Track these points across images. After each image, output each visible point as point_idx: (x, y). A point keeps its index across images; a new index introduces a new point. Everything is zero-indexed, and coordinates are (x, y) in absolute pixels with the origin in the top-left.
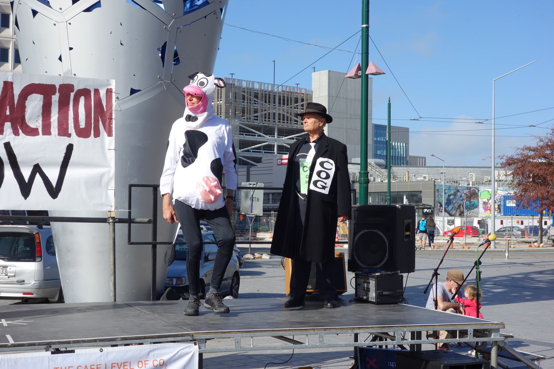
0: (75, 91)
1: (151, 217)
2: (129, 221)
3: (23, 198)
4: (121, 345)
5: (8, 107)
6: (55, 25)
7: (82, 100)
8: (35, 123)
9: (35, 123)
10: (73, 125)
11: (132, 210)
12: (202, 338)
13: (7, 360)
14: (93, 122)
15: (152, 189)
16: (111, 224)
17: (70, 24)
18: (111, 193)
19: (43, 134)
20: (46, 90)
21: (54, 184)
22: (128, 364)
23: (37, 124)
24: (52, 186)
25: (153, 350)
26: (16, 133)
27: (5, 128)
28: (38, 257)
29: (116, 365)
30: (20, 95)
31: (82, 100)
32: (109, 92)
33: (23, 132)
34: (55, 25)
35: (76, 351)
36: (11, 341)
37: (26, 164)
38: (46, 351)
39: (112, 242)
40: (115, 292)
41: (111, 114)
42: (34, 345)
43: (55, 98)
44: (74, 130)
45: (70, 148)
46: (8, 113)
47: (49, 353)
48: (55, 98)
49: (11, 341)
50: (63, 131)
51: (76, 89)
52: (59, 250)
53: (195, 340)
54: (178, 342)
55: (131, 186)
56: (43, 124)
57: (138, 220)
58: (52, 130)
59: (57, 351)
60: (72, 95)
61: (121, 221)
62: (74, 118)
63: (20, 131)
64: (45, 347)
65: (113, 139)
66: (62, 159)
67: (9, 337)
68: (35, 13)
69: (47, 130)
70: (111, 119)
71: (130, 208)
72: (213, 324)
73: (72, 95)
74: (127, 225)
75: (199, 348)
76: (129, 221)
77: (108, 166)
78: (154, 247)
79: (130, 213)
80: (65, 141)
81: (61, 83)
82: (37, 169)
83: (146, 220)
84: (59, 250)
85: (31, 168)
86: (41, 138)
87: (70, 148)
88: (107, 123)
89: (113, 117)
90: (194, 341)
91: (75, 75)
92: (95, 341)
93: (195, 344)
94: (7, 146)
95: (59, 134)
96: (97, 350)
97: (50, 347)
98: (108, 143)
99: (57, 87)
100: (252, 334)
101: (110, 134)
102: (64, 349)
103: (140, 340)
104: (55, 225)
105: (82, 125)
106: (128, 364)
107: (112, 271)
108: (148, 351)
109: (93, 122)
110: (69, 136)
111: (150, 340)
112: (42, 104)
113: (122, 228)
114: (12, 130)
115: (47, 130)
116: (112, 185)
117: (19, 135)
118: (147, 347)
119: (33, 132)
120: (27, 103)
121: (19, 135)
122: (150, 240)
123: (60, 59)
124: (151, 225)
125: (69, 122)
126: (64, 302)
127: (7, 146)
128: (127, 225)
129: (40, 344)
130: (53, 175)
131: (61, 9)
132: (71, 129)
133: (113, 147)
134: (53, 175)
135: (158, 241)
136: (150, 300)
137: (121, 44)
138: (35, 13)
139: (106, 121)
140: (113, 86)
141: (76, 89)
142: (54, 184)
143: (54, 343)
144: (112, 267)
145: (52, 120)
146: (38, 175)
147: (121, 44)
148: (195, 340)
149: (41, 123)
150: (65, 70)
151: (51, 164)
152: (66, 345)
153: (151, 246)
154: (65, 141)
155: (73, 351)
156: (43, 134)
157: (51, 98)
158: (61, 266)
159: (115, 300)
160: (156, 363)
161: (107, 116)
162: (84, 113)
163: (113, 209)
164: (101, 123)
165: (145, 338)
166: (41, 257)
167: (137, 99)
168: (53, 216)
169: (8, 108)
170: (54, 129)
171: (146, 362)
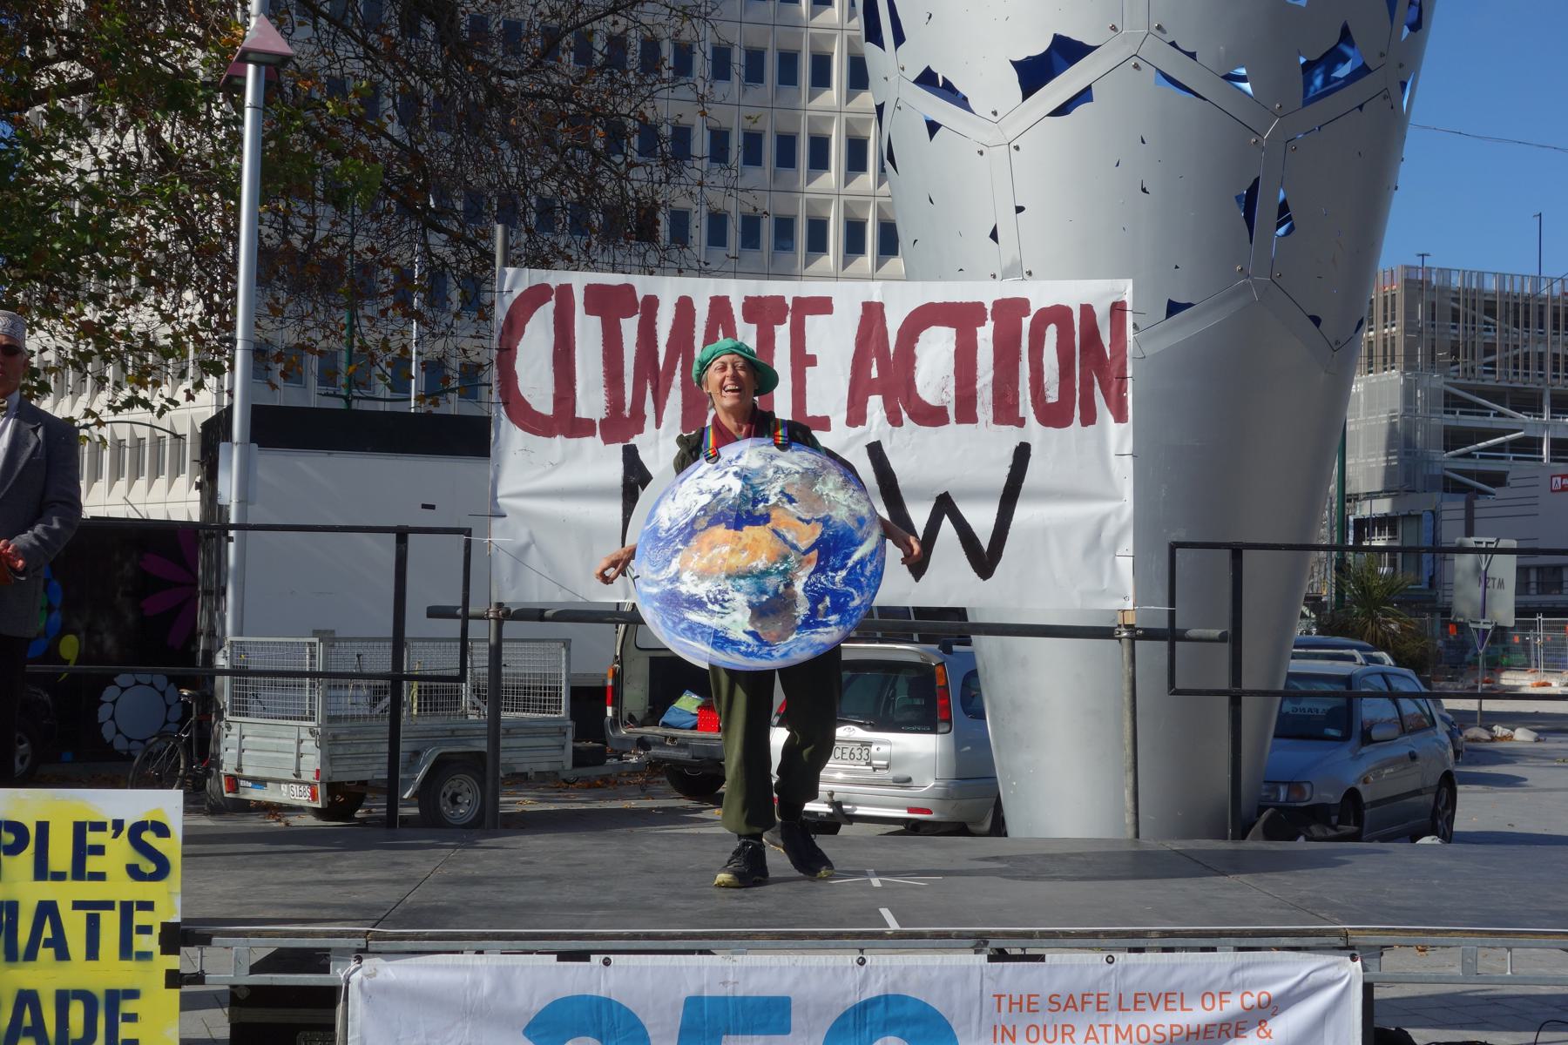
0: (1033, 313)
1: (1227, 628)
2: (1171, 635)
3: (910, 577)
4: (1152, 949)
5: (875, 360)
6: (981, 153)
7: (1051, 332)
10: (1029, 398)
11: (1177, 609)
12: (1372, 943)
13: (885, 968)
14: (1077, 386)
15: (1227, 553)
16: (1125, 641)
17: (1017, 148)
18: (1126, 564)
19: (958, 422)
20: (962, 317)
21: (985, 542)
22: (1177, 998)
24: (980, 547)
25: (1243, 967)
26: (895, 421)
28: (943, 721)
29: (1146, 998)
30: (900, 332)
31: (1051, 332)
32: (1118, 309)
33: (911, 416)
34: (981, 153)
35: (1048, 957)
36: (894, 926)
37: (919, 496)
38: (976, 952)
39: (1126, 687)
40: (1137, 814)
41: (1123, 366)
42: (947, 935)
43: (985, 334)
44: (1031, 410)
45: (1022, 454)
46: (874, 373)
47: (983, 958)
48: (985, 334)
49: (894, 926)
50: (1006, 413)
51: (1034, 309)
52: (994, 707)
53: (1352, 948)
54: (1306, 949)
55: (1174, 547)
56: (957, 397)
57: (1193, 633)
58: (979, 411)
59: (1000, 956)
60: (1026, 322)
61: (1150, 635)
62: (1031, 380)
63: (905, 415)
64: (972, 942)
65: (1128, 427)
66: (1002, 480)
67: (886, 913)
68: (933, 127)
69: (967, 413)
70: (1123, 378)
71: (1172, 603)
72: (1398, 908)
73: (1026, 322)
74: (1165, 644)
75: (1365, 969)
76: (1171, 635)
77: (1118, 497)
78: (1236, 702)
79: (1172, 615)
80: (1010, 437)
81: (999, 297)
82: (945, 505)
83: (1216, 633)
84: (994, 707)
85: (932, 503)
86: (952, 429)
87: (1022, 454)
88: (1113, 389)
89: (1129, 373)
90: (1349, 949)
91: (1030, 273)
92: (1095, 935)
93: (1353, 958)
94: (875, 451)
95: (997, 420)
96: (1099, 958)
97: (986, 943)
98: (1116, 438)
99: (989, 307)
100: (1510, 941)
101: (1120, 417)
102: (1018, 952)
103: (1206, 941)
104: (985, 646)
105: (1052, 395)
106: (1177, 998)
107: (1128, 762)
108: (1228, 968)
109: (1077, 386)
110: (1021, 423)
111: (1234, 941)
112: (953, 347)
113: (1153, 654)
115: (967, 413)
116: (1128, 545)
118: (1224, 960)
119: (931, 416)
120: (919, 349)
121: (901, 424)
122: (1225, 684)
123: (994, 235)
124: (1225, 649)
125: (1020, 389)
126: (1006, 835)
127: (875, 451)
128: (1165, 644)
129: (960, 936)
130: (982, 519)
131: (995, 113)
132: (1026, 408)
133: (1128, 447)
134: (982, 519)
135: (1247, 684)
136: (1225, 838)
137: (1144, 190)
138: (933, 127)
139: (1110, 384)
140: (1128, 298)
141: (1034, 309)
142: (985, 542)
143: (995, 935)
144: (1128, 750)
145: (979, 386)
146: (946, 523)
147: (1144, 190)
148: (1352, 948)
149: (953, 394)
150: (1007, 262)
151: (977, 495)
152: (1023, 942)
153: (1226, 699)
154: (1010, 437)
155: (1041, 958)
156: (958, 422)
157: (975, 334)
158: (998, 747)
159: (1137, 835)
160: (1250, 1001)
161: (1114, 370)
162: (1056, 365)
163: (1129, 605)
164: (1097, 389)
165: (1221, 934)
166: (949, 721)
167: (1185, 329)
168: (980, 620)
170: (984, 408)
171: (1225, 997)
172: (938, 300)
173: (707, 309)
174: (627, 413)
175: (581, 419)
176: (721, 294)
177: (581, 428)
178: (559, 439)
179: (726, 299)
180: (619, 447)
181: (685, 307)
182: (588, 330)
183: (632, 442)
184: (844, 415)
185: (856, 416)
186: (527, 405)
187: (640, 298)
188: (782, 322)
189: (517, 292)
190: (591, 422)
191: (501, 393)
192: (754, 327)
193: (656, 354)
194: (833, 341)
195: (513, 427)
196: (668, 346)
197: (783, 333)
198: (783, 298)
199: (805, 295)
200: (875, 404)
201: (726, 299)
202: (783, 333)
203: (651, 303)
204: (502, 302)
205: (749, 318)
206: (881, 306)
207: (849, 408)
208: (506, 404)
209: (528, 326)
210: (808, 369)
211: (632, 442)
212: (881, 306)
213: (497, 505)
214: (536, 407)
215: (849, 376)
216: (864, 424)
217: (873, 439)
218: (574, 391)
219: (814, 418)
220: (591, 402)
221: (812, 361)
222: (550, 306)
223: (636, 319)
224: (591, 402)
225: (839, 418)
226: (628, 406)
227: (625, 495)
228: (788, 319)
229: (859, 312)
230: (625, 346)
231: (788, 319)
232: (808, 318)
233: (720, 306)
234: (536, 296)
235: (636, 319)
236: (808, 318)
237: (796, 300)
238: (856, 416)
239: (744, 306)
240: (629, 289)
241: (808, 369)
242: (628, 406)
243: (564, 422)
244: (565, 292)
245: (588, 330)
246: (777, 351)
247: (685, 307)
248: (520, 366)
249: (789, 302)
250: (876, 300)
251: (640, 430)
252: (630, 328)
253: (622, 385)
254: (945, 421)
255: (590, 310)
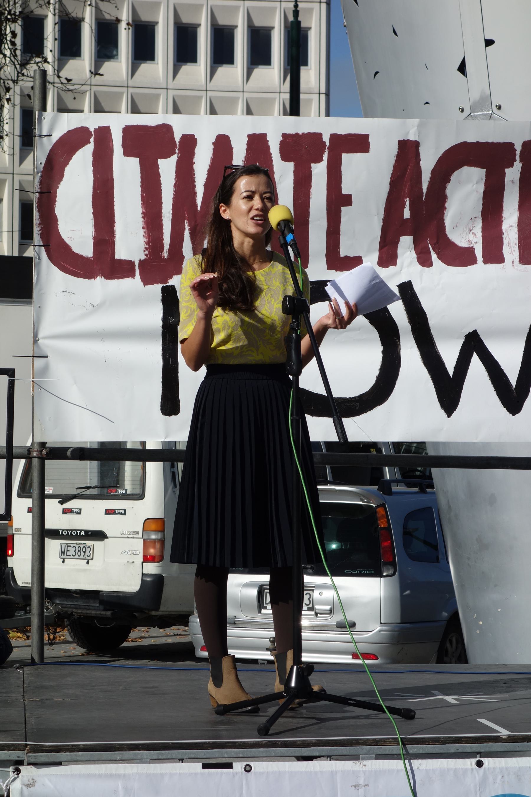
5: (407, 200)
8: (465, 233)
9: (465, 233)
23: (471, 237)
26: (424, 261)
27: (400, 251)
46: (407, 214)
63: (434, 256)
69: (494, 254)
114: (415, 255)
115: (494, 254)
117: (430, 265)
121: (430, 265)
169: (407, 204)
172: (471, 139)
173: (245, 146)
174: (165, 254)
175: (120, 261)
176: (258, 132)
177: (120, 270)
178: (100, 280)
179: (264, 136)
180: (157, 289)
181: (222, 144)
182: (126, 171)
183: (171, 282)
184: (375, 256)
185: (388, 257)
186: (67, 247)
187: (177, 138)
188: (319, 160)
189: (56, 136)
190: (131, 264)
191: (42, 236)
192: (291, 166)
193: (194, 194)
194: (367, 177)
195: (56, 271)
196: (206, 186)
197: (319, 171)
198: (320, 135)
199: (341, 131)
200: (406, 242)
201: (264, 136)
202: (319, 171)
203: (189, 142)
204: (42, 144)
205: (285, 157)
206: (416, 144)
207: (381, 249)
208: (46, 246)
209: (68, 170)
210: (343, 209)
211: (171, 282)
212: (416, 144)
213: (38, 347)
214: (76, 249)
215: (382, 216)
216: (395, 264)
217: (404, 279)
218: (113, 232)
219: (347, 258)
220: (130, 243)
221: (347, 200)
222: (88, 150)
223: (174, 159)
224: (130, 243)
225: (371, 260)
226: (166, 247)
227: (164, 336)
228: (325, 157)
229: (394, 149)
230: (163, 187)
231: (325, 157)
232: (344, 156)
233: (257, 143)
234: (74, 140)
235: (174, 159)
236: (344, 156)
237: (334, 137)
238: (388, 257)
239: (282, 143)
240: (166, 129)
241: (343, 209)
242: (166, 247)
243: (104, 263)
244: (104, 134)
245: (126, 171)
246: (313, 190)
247: (222, 144)
248: (60, 209)
249: (326, 139)
250: (412, 137)
251: (179, 271)
252: (167, 168)
253: (160, 227)
254: (473, 261)
255: (128, 152)
